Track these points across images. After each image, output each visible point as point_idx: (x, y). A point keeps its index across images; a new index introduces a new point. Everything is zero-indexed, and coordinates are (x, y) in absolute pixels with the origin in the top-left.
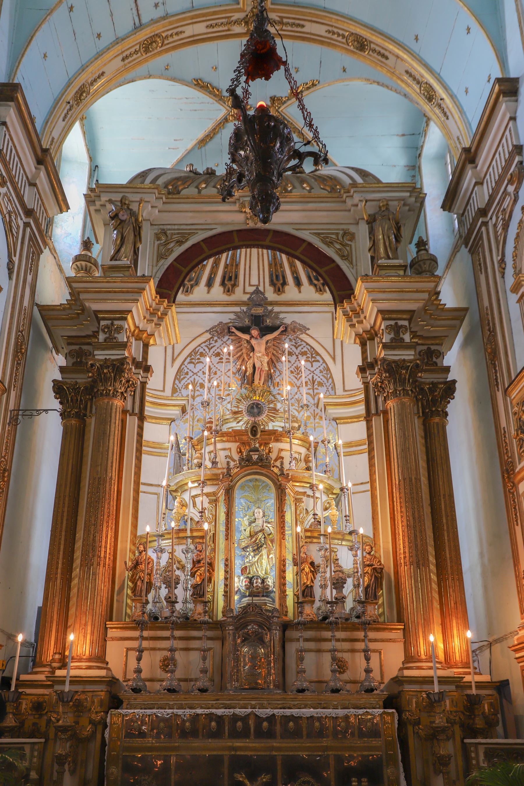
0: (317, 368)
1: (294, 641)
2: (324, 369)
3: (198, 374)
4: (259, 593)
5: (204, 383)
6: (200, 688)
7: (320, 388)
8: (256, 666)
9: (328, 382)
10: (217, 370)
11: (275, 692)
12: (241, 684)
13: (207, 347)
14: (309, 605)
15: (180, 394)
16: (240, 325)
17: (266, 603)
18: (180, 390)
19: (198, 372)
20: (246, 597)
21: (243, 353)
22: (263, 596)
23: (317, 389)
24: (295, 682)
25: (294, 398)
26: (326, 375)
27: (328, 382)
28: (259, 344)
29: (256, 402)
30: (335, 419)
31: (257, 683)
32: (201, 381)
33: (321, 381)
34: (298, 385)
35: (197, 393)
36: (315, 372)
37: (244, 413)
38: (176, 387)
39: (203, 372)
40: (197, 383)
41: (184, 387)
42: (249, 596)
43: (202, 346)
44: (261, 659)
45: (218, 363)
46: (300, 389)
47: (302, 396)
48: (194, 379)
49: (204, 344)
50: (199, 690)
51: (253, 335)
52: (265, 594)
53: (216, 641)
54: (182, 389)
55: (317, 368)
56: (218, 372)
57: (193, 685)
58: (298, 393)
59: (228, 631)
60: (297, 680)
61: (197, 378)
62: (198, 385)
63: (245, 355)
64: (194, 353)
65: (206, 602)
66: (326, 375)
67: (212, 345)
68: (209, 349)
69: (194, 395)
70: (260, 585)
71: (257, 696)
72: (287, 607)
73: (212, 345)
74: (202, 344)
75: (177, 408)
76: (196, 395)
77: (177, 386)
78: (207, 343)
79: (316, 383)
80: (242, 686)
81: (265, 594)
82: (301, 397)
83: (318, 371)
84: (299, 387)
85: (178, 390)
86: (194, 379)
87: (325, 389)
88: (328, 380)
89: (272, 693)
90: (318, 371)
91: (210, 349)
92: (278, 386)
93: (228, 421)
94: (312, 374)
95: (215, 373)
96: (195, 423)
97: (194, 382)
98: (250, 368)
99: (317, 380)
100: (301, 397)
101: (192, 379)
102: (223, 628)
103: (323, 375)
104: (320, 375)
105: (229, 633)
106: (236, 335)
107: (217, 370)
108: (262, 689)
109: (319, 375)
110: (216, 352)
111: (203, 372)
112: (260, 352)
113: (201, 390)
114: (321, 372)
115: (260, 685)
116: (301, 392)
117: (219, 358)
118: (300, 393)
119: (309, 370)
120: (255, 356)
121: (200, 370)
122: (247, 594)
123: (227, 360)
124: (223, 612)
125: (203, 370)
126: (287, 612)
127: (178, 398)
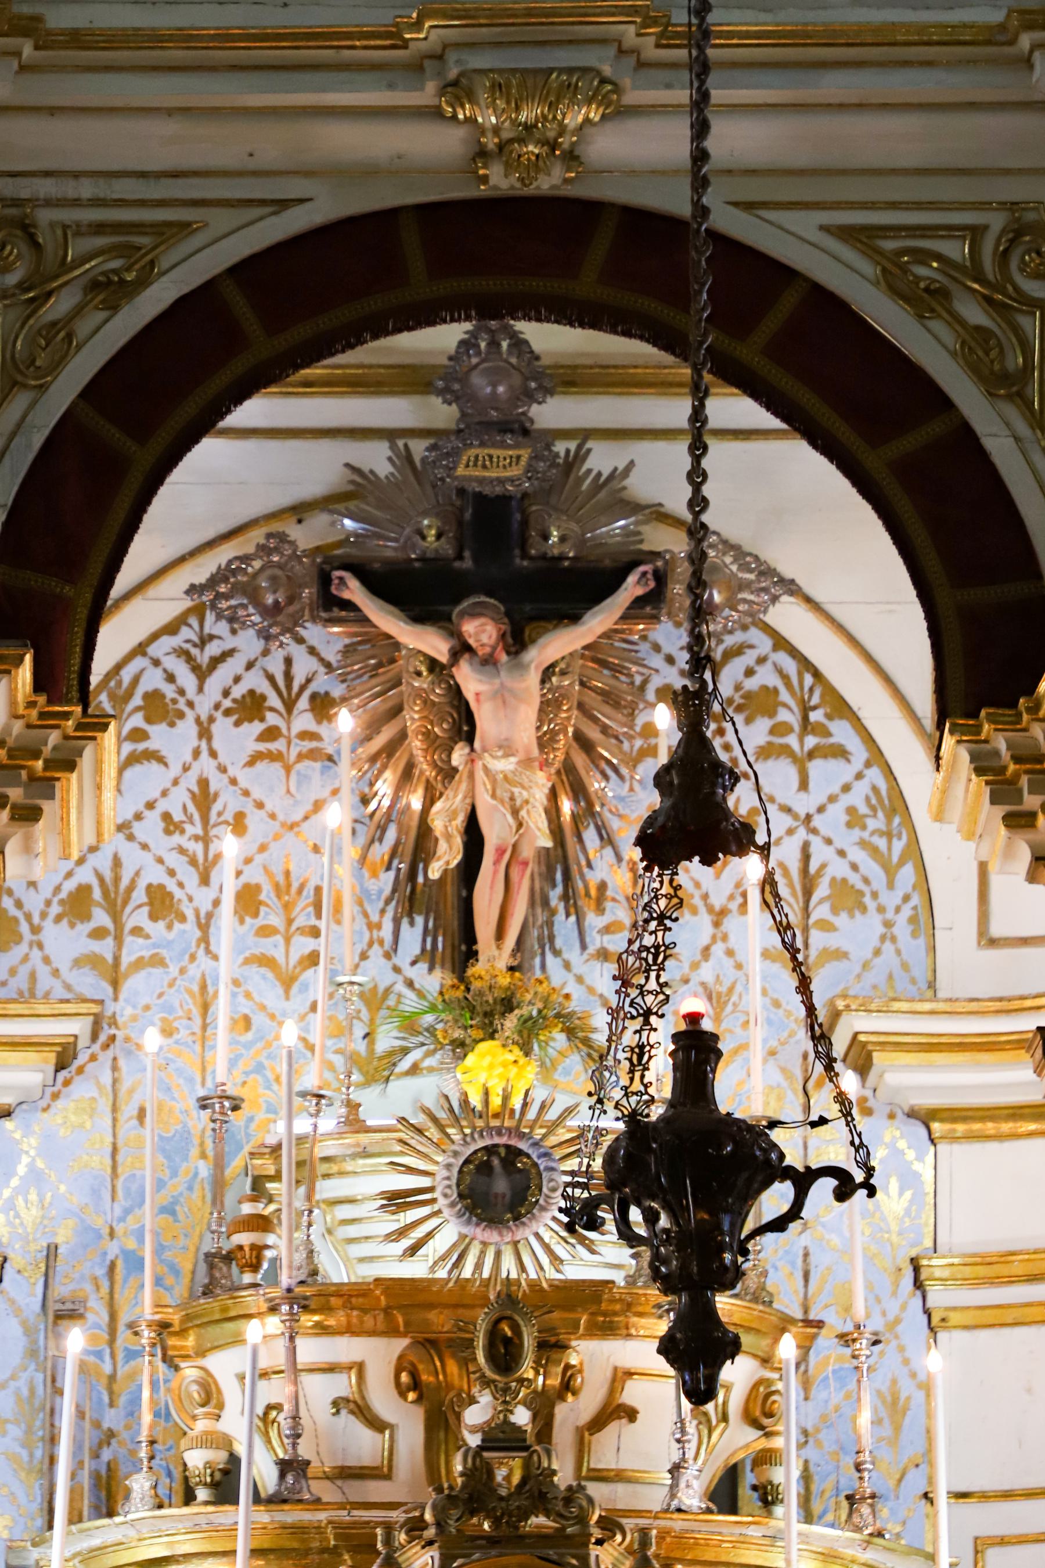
0: (832, 799)
2: (874, 801)
3: (137, 828)
5: (171, 885)
7: (842, 920)
9: (891, 885)
10: (249, 809)
13: (189, 658)
15: (36, 954)
16: (388, 549)
18: (35, 930)
19: (138, 817)
21: (402, 736)
23: (826, 926)
25: (695, 978)
26: (881, 843)
27: (891, 885)
28: (503, 698)
29: (503, 1140)
30: (925, 1117)
32: (154, 875)
33: (854, 879)
34: (717, 902)
35: (133, 949)
36: (817, 821)
37: (442, 1202)
38: (13, 911)
39: (167, 817)
40: (131, 888)
41: (55, 909)
43: (153, 650)
45: (251, 762)
46: (730, 924)
47: (739, 966)
48: (117, 862)
49: (168, 642)
51: (472, 642)
54: (48, 925)
55: (832, 799)
56: (255, 820)
58: (718, 949)
61: (132, 858)
62: (139, 896)
63: (416, 744)
64: (112, 697)
66: (881, 843)
67: (213, 649)
68: (196, 669)
69: (117, 959)
73: (213, 649)
74: (154, 637)
75: (31, 1056)
76: (126, 960)
77: (19, 904)
78: (185, 633)
79: (822, 890)
82: (730, 974)
83: (837, 813)
84: (723, 912)
85: (24, 928)
86: (117, 862)
87: (870, 925)
88: (890, 872)
90: (837, 813)
91: (202, 673)
92: (600, 910)
93: (334, 1168)
94: (802, 834)
95: (239, 824)
96: (128, 1126)
97: (117, 879)
98: (448, 837)
99: (830, 872)
100: (730, 974)
101: (102, 861)
103: (863, 844)
104: (847, 839)
106: (365, 620)
107: (249, 809)
109: (838, 844)
110: (238, 692)
111: (167, 817)
112: (507, 749)
113: (157, 929)
114: (854, 819)
116: (733, 942)
117: (257, 727)
118: (730, 953)
119: (787, 810)
120: (480, 774)
121: (150, 806)
123: (308, 745)
125: (162, 806)
127: (42, 1009)
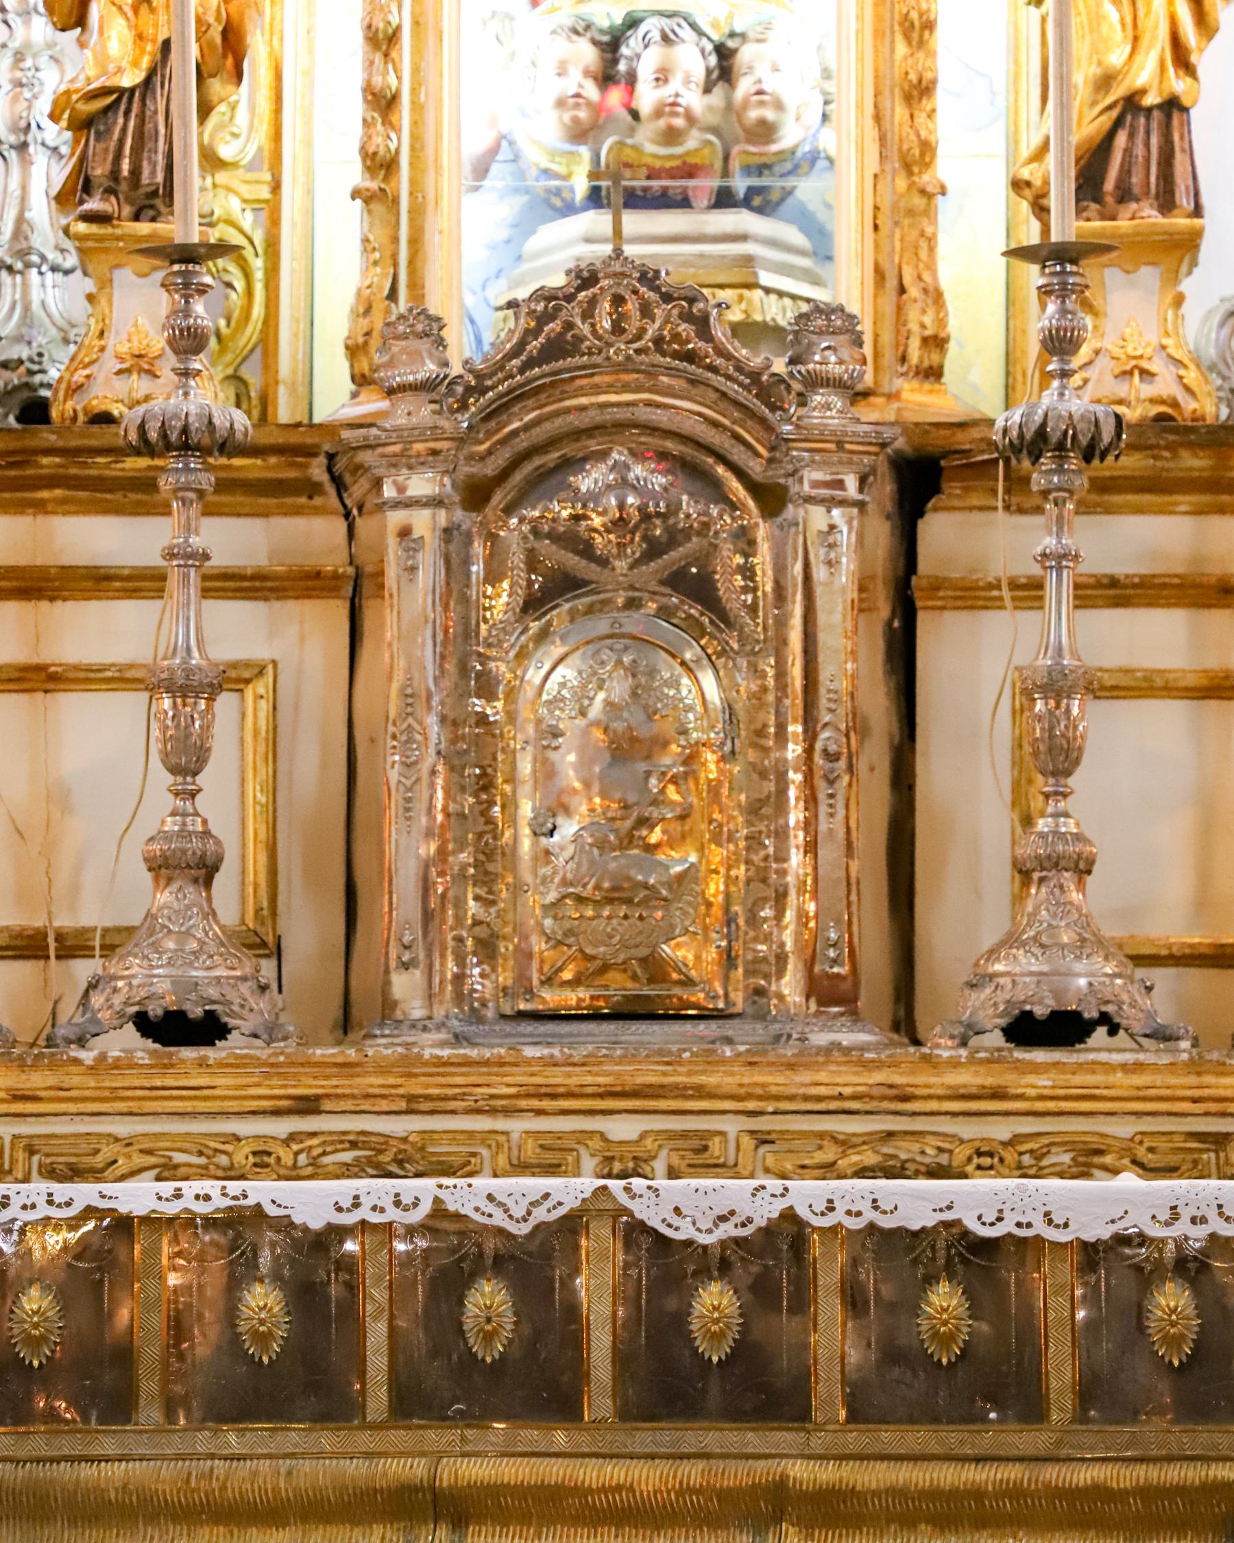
1: (995, 604)
4: (690, 171)
6: (155, 1010)
8: (645, 822)
11: (821, 1038)
12: (522, 977)
14: (1148, 275)
17: (748, 261)
20: (569, 209)
22: (724, 199)
24: (992, 954)
31: (655, 968)
42: (596, 198)
44: (691, 759)
50: (144, 1024)
52: (740, 185)
53: (292, 607)
57: (92, 986)
59: (396, 518)
60: (1011, 940)
65: (187, 255)
70: (694, 100)
71: (650, 1075)
72: (936, 297)
80: (530, 992)
81: (740, 185)
89: (789, 1052)
102: (358, 489)
105: (405, 533)
108: (705, 1016)
115: (688, 982)
122: (581, 186)
124: (354, 351)
126: (937, 342)
